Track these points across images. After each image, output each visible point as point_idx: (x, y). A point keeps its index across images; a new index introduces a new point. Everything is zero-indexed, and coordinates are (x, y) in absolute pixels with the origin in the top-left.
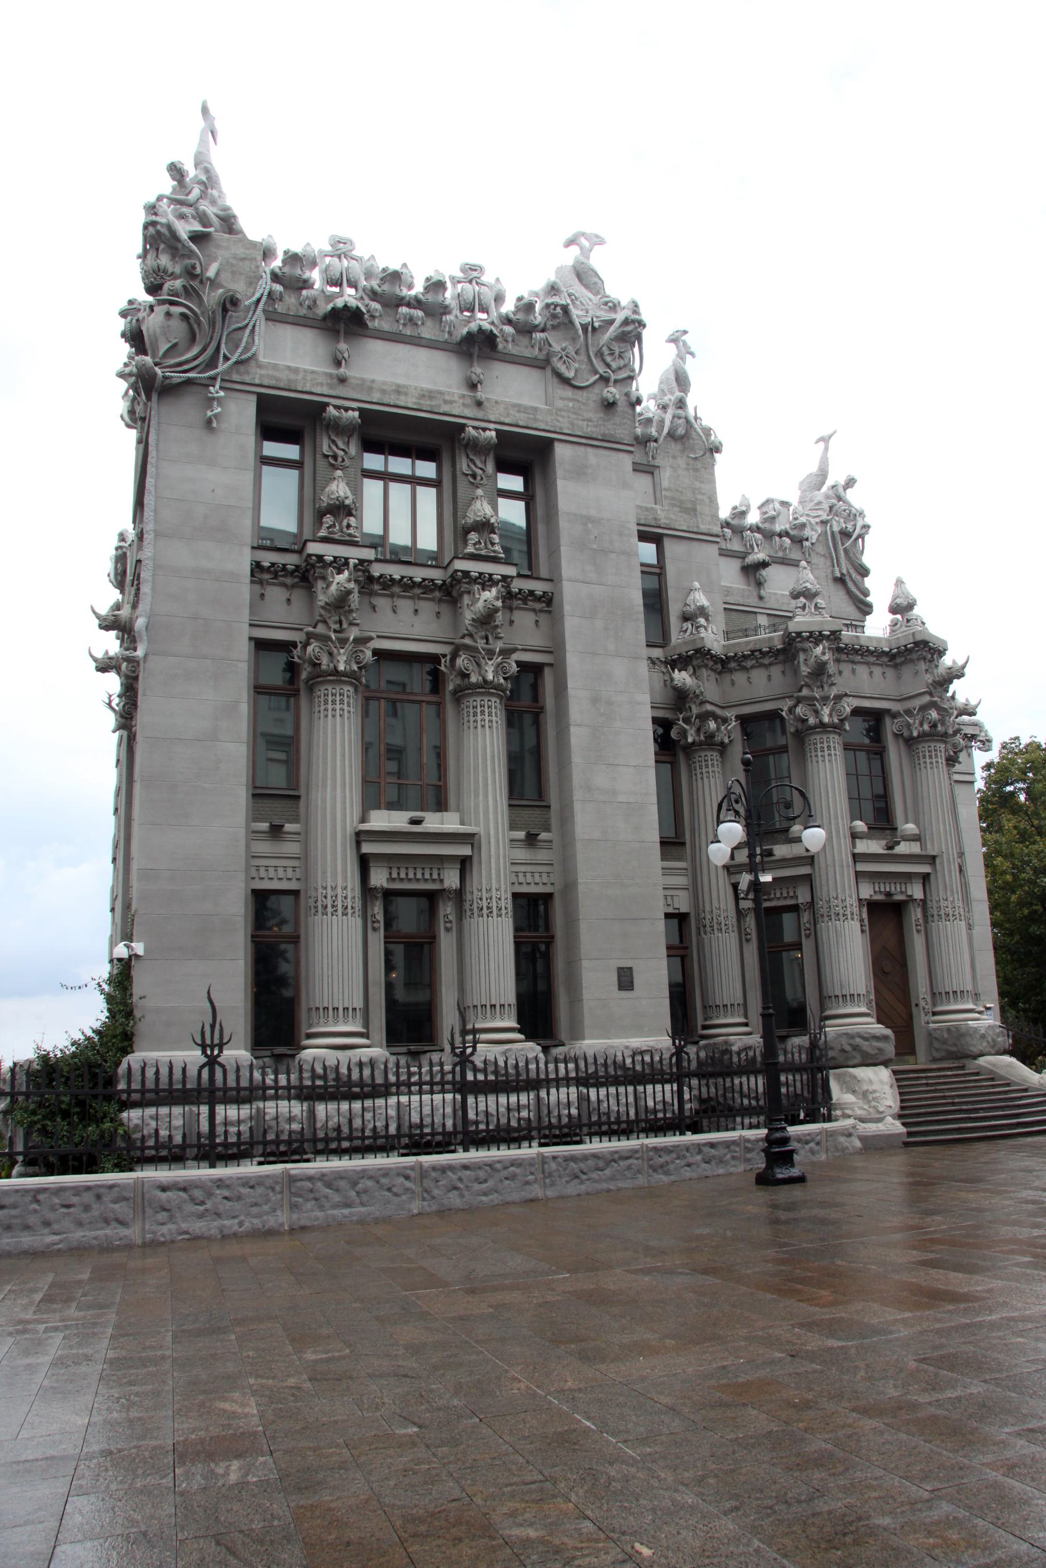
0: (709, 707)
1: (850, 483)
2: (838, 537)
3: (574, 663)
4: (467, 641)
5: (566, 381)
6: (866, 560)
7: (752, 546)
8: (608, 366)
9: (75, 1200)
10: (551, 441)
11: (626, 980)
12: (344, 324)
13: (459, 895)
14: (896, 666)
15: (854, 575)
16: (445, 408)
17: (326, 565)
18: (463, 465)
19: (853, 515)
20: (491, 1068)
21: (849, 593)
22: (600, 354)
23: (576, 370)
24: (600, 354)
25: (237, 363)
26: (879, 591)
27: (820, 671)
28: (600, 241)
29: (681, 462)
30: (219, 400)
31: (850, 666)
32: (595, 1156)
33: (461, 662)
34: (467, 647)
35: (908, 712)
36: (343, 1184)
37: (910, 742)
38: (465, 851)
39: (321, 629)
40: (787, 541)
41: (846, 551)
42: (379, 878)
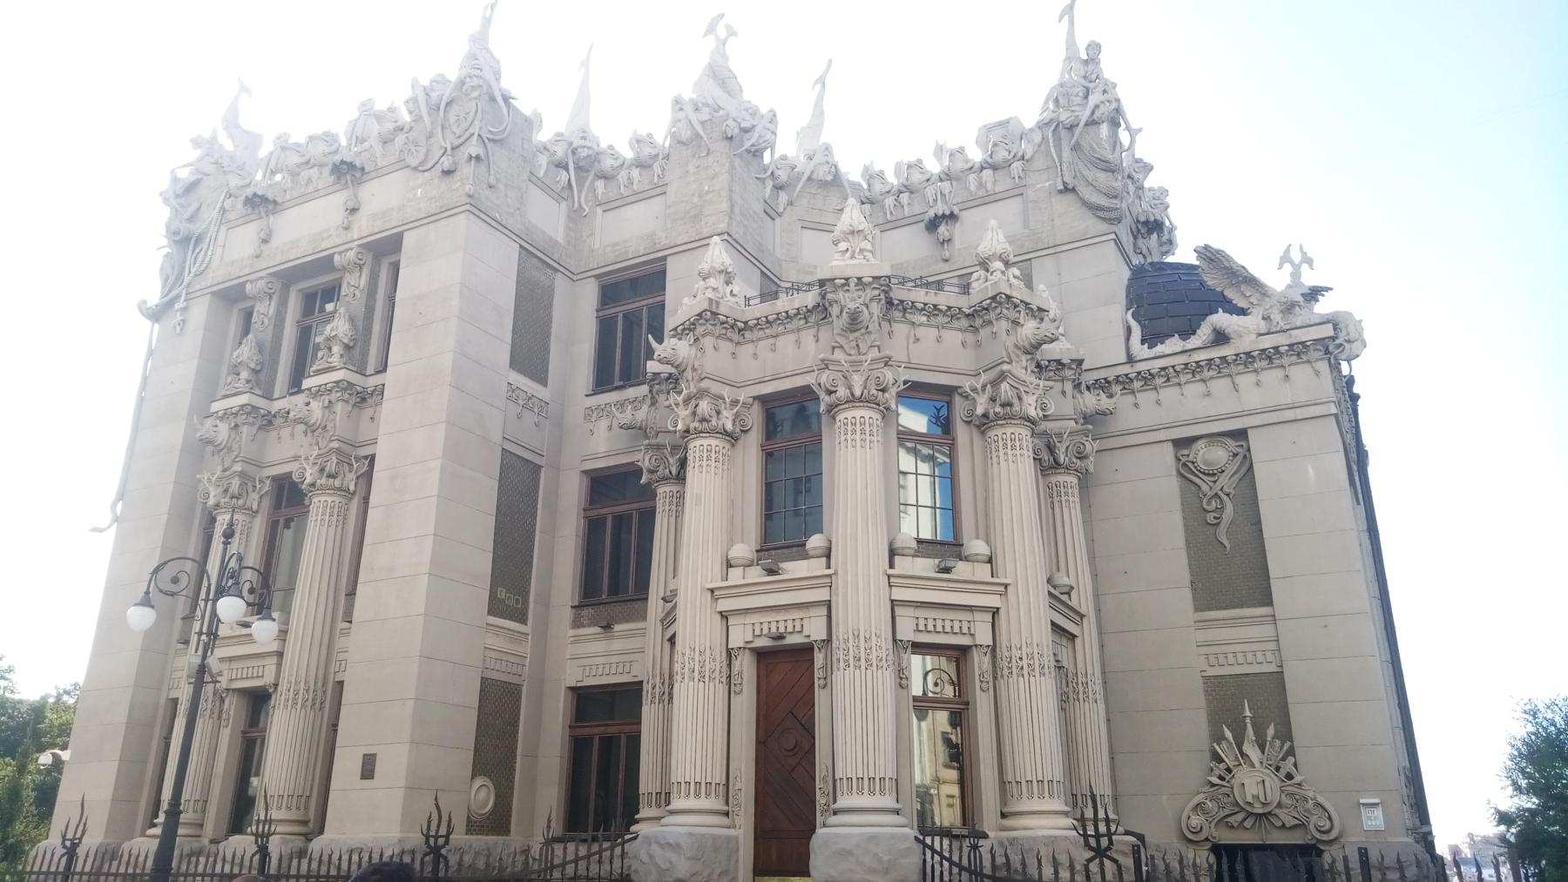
0: (660, 440)
1: (1094, 48)
2: (1063, 133)
5: (415, 169)
7: (935, 201)
10: (402, 233)
11: (368, 769)
15: (1090, 175)
16: (324, 245)
20: (237, 861)
21: (1086, 204)
23: (427, 155)
29: (691, 169)
30: (185, 309)
31: (771, 341)
40: (987, 173)
41: (1076, 148)
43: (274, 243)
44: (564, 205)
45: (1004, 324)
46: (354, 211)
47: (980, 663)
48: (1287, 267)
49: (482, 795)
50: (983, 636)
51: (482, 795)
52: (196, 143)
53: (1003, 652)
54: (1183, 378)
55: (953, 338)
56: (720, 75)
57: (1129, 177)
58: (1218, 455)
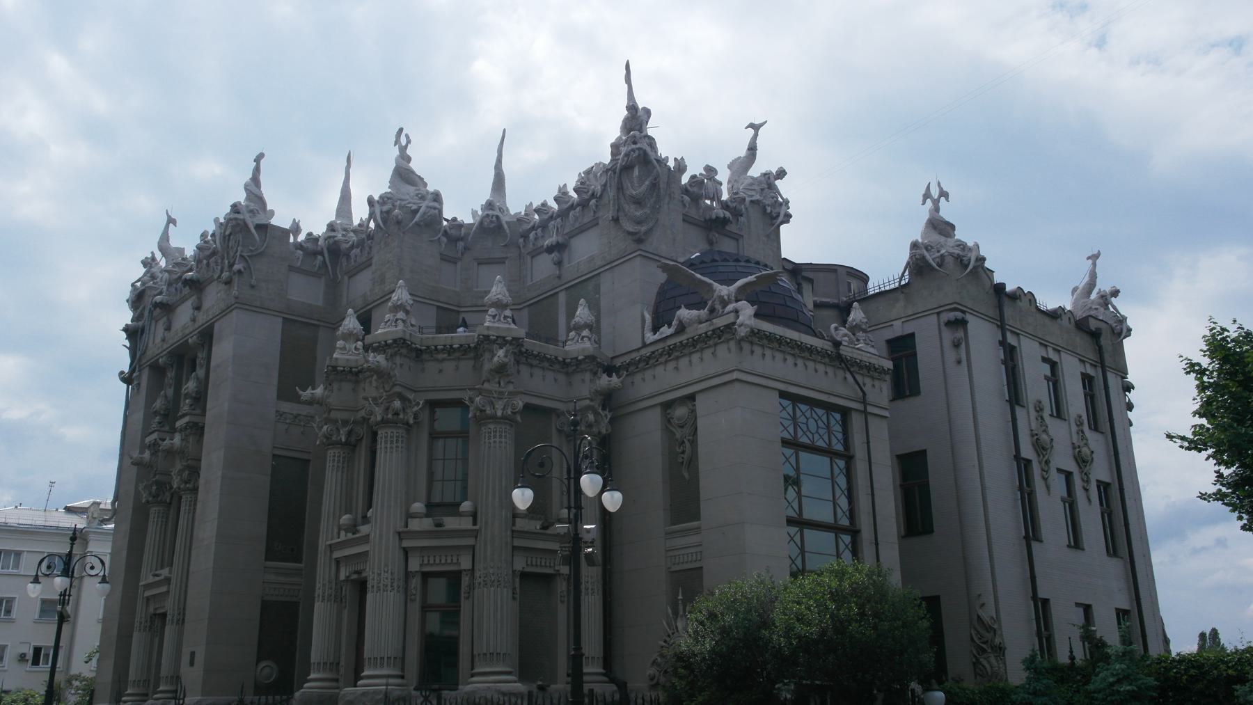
12: (167, 309)
16: (187, 332)
41: (620, 188)
43: (174, 329)
44: (323, 279)
45: (487, 355)
46: (198, 308)
47: (465, 580)
48: (929, 201)
49: (268, 670)
50: (465, 563)
51: (268, 670)
52: (145, 263)
53: (477, 574)
54: (663, 359)
55: (466, 365)
56: (404, 174)
57: (685, 190)
58: (680, 412)
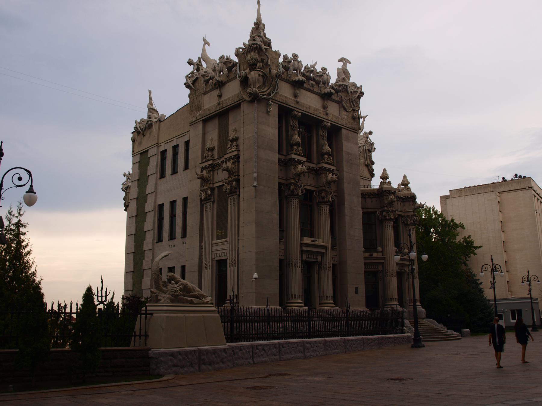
1: (371, 133)
3: (346, 197)
4: (324, 188)
5: (345, 110)
6: (373, 159)
8: (354, 106)
9: (294, 346)
13: (320, 264)
14: (403, 202)
17: (296, 162)
18: (321, 132)
19: (372, 144)
21: (369, 170)
22: (352, 102)
24: (352, 102)
25: (276, 93)
26: (378, 170)
27: (391, 203)
28: (350, 63)
32: (371, 339)
33: (323, 194)
34: (325, 191)
35: (408, 216)
36: (334, 344)
37: (406, 225)
38: (324, 251)
39: (293, 181)
42: (305, 257)
